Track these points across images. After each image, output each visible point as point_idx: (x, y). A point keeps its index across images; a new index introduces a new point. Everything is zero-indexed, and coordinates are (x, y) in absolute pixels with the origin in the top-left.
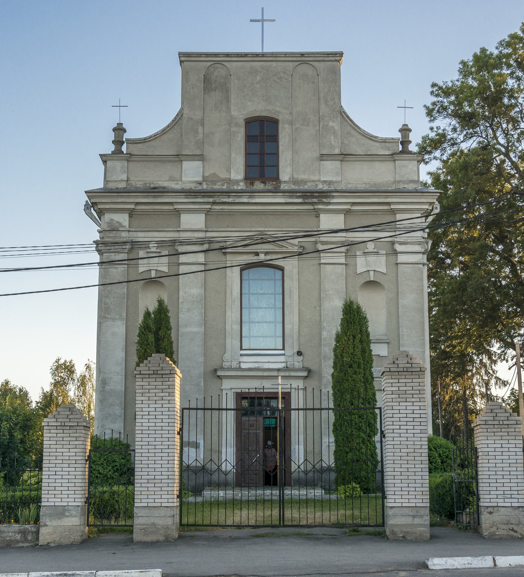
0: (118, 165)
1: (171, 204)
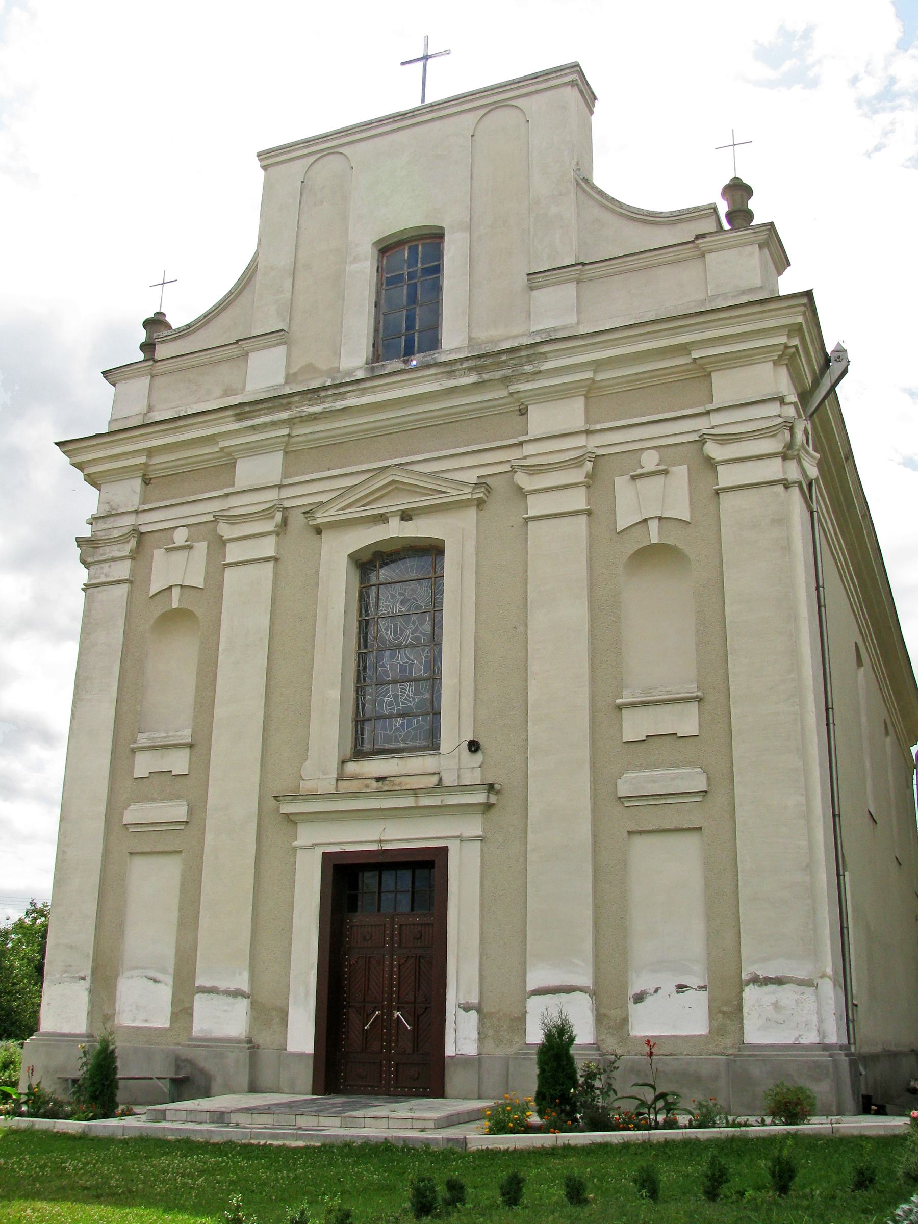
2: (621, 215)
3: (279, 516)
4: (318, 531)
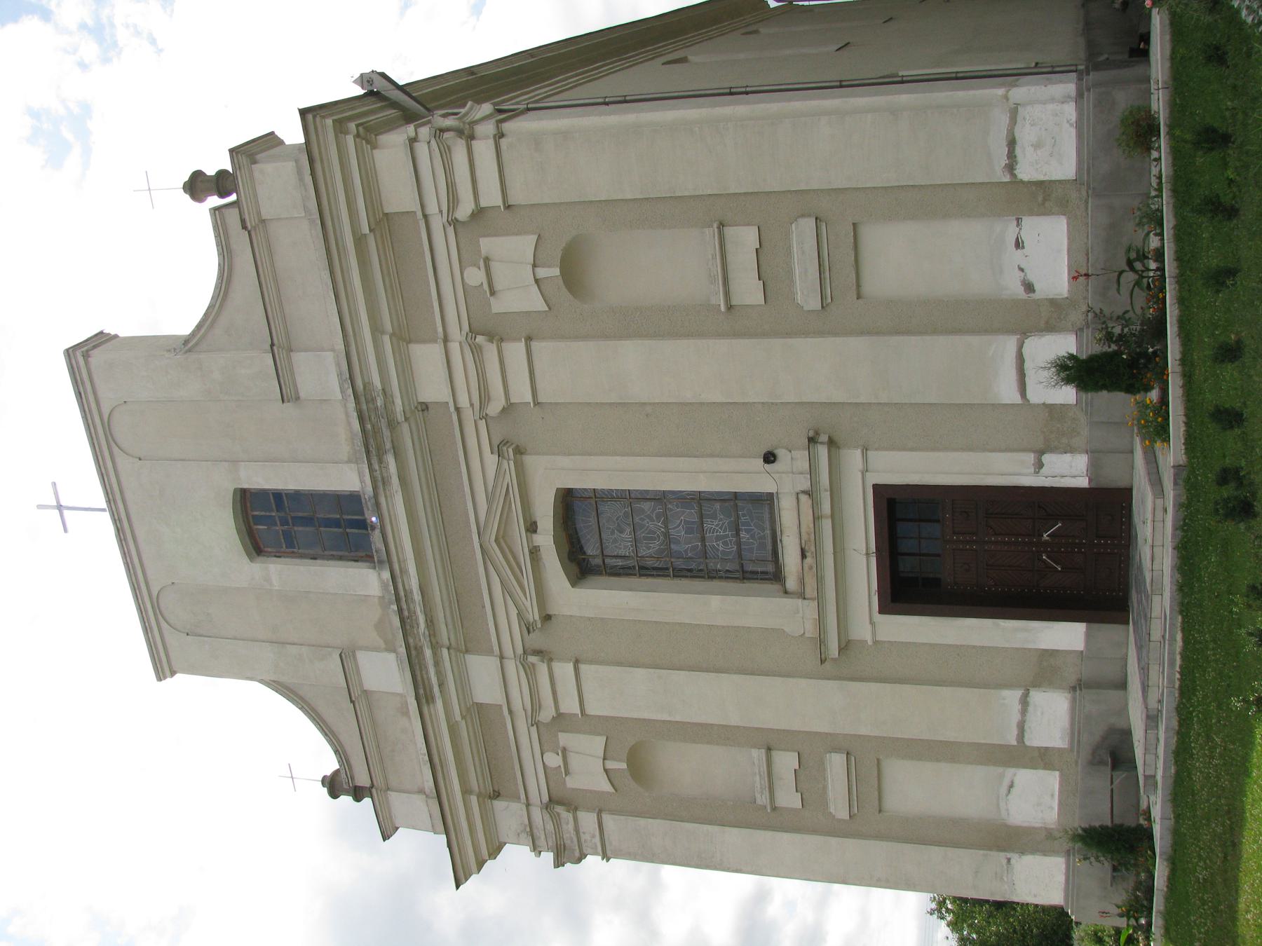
1: (453, 729)
2: (221, 306)
3: (532, 659)
4: (547, 618)
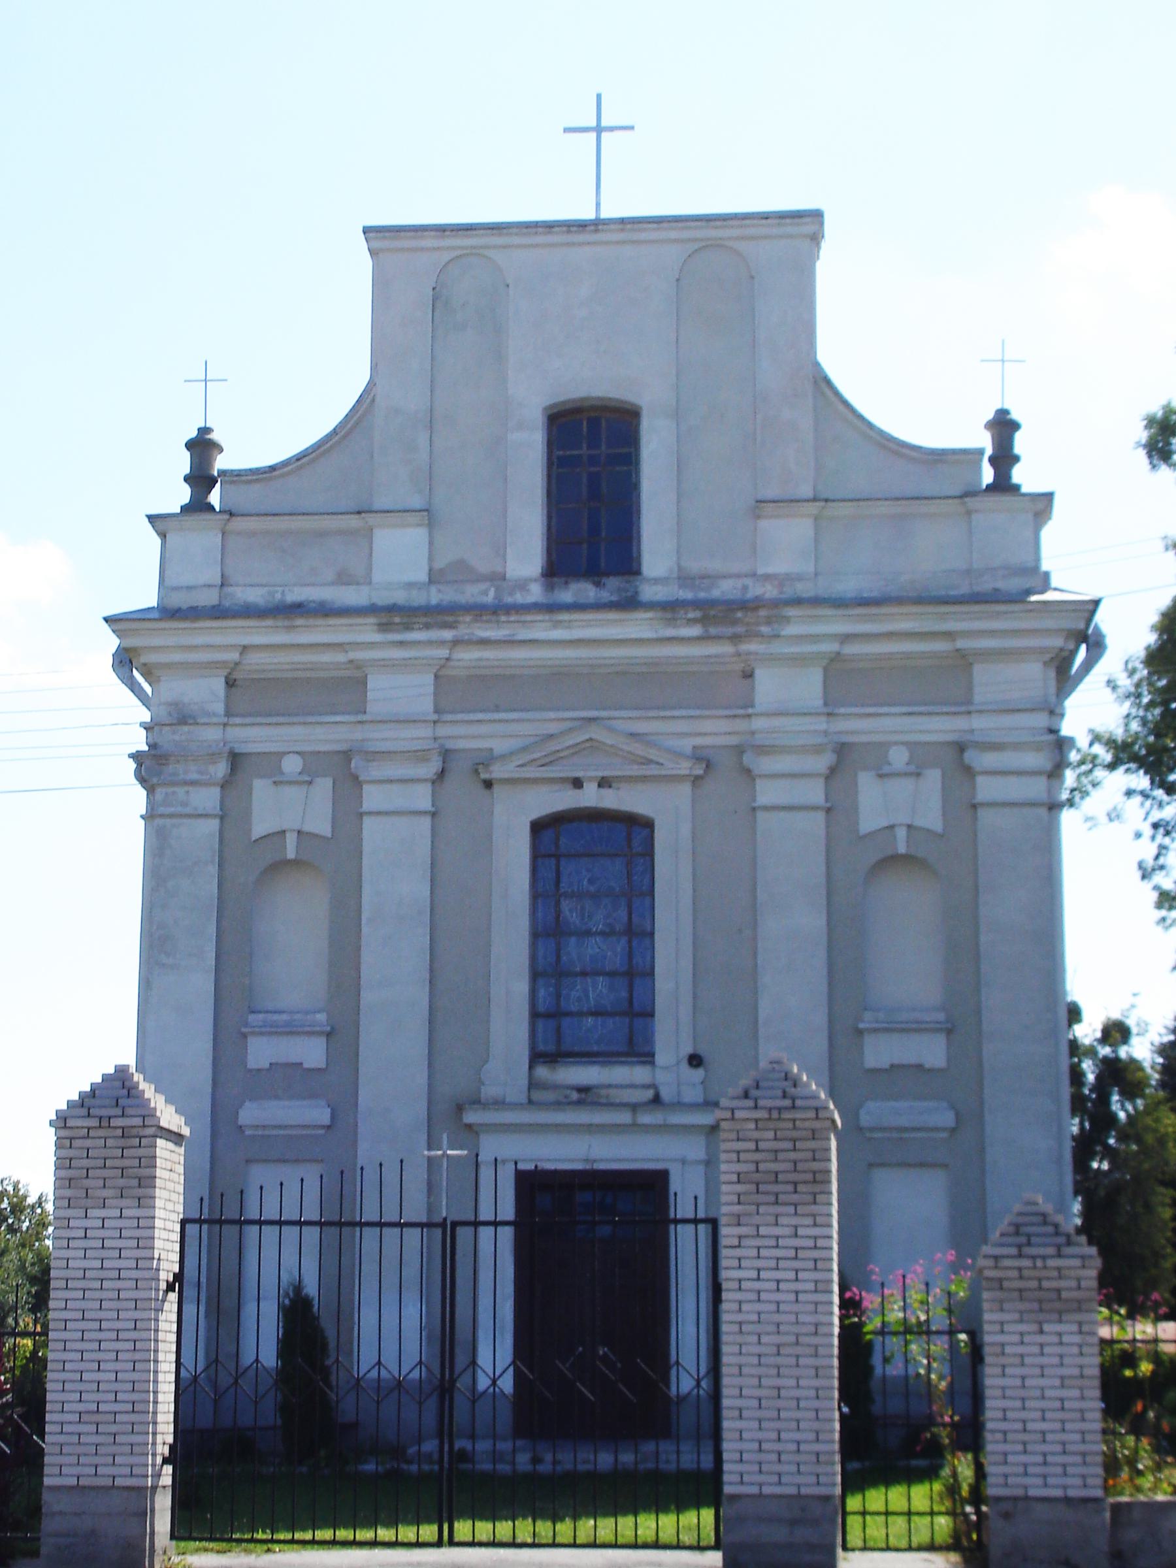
0: (203, 539)
1: (340, 647)
4: (488, 784)
